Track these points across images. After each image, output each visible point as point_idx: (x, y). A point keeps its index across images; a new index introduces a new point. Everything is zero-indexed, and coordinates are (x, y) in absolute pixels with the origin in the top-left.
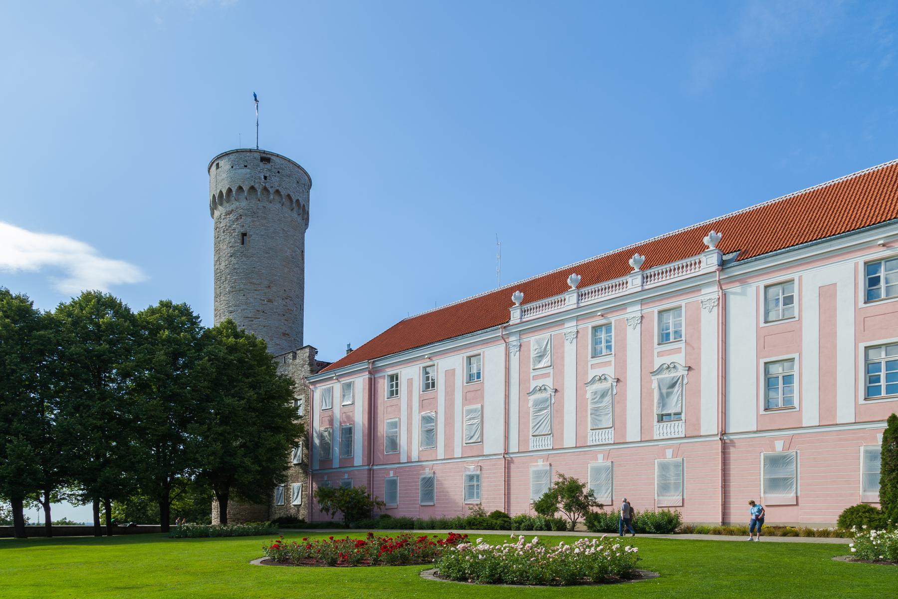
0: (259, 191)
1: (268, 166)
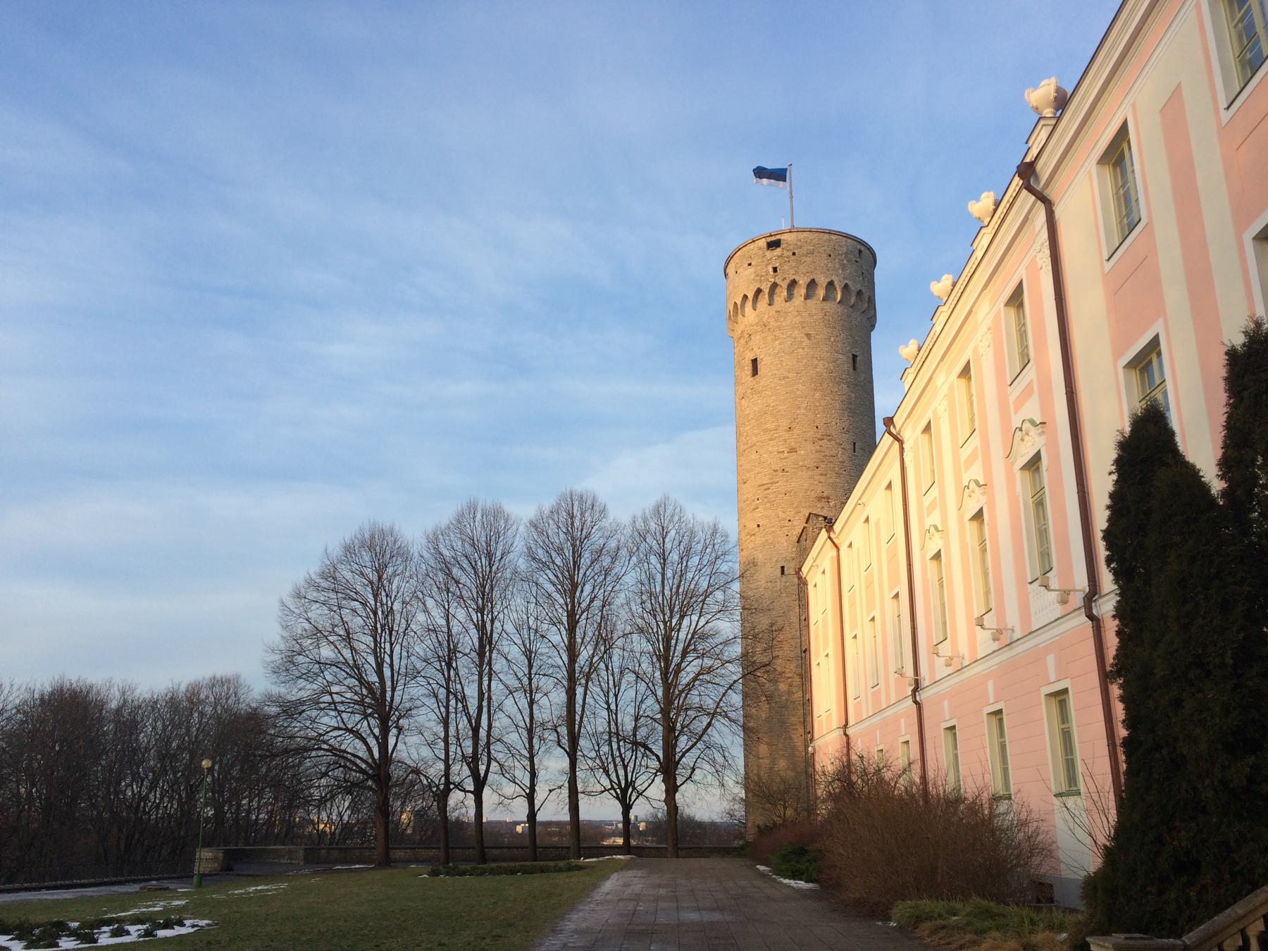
1: (778, 251)
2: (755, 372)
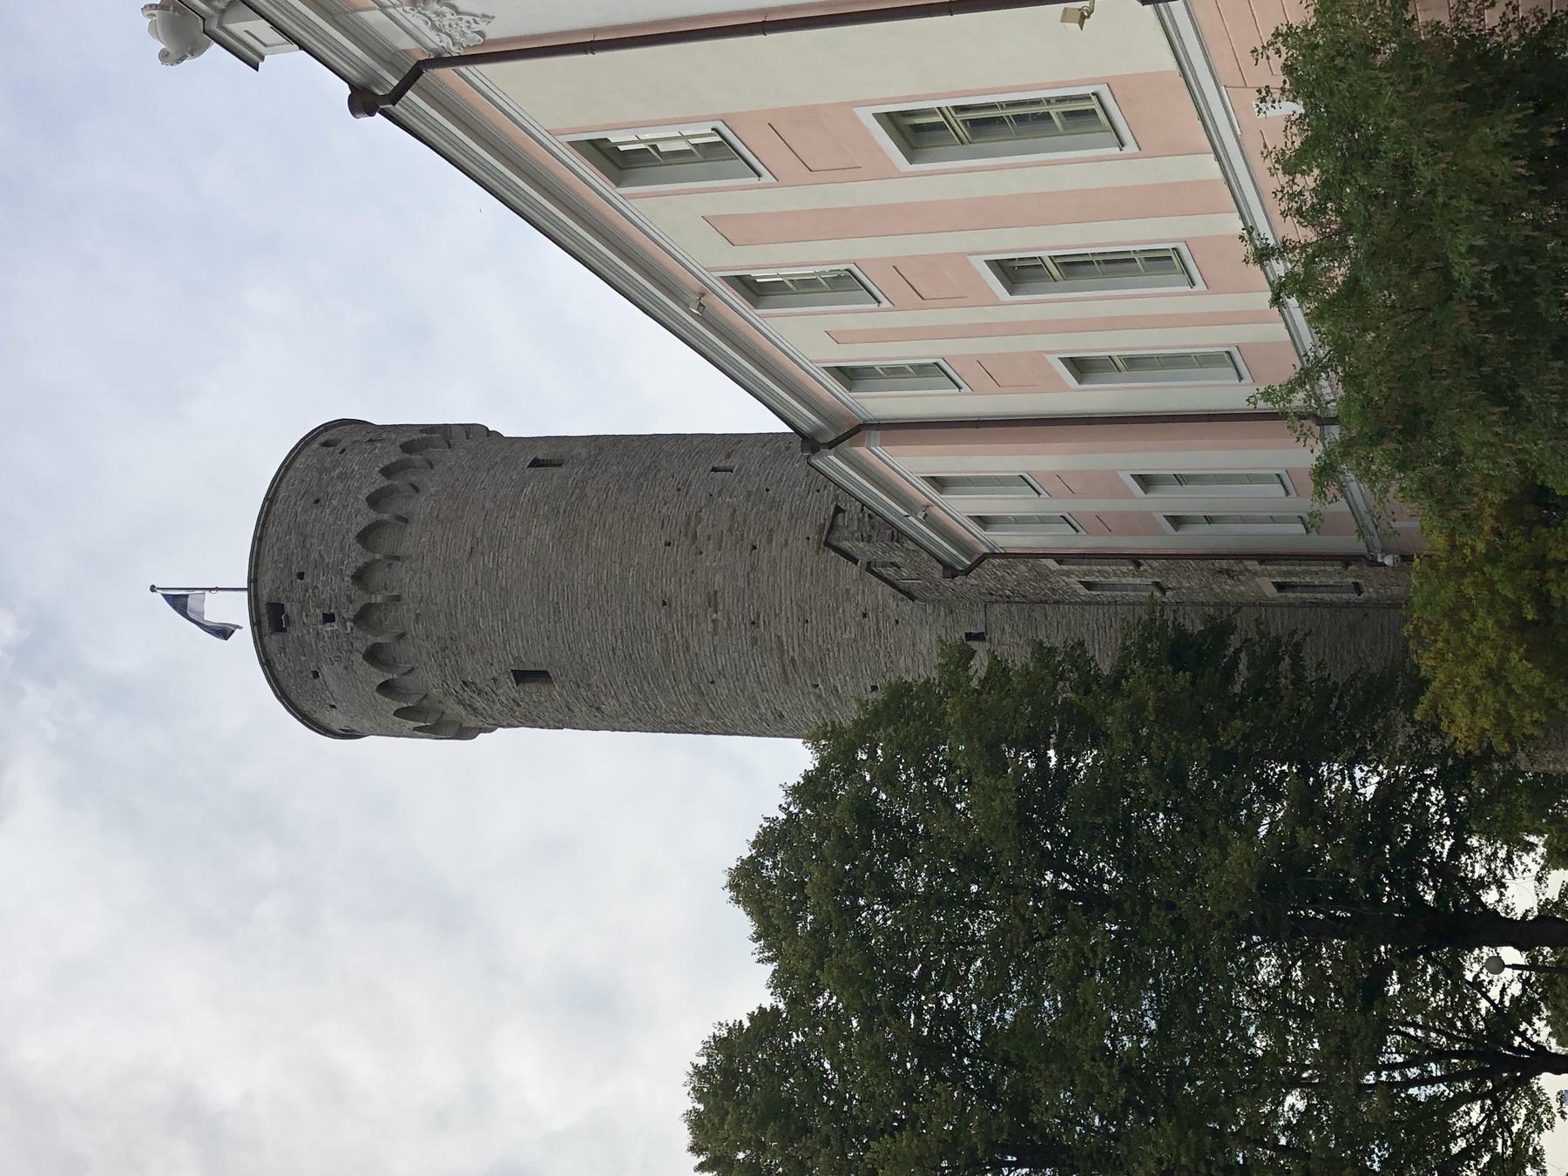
0: (372, 639)
1: (291, 609)
2: (541, 676)
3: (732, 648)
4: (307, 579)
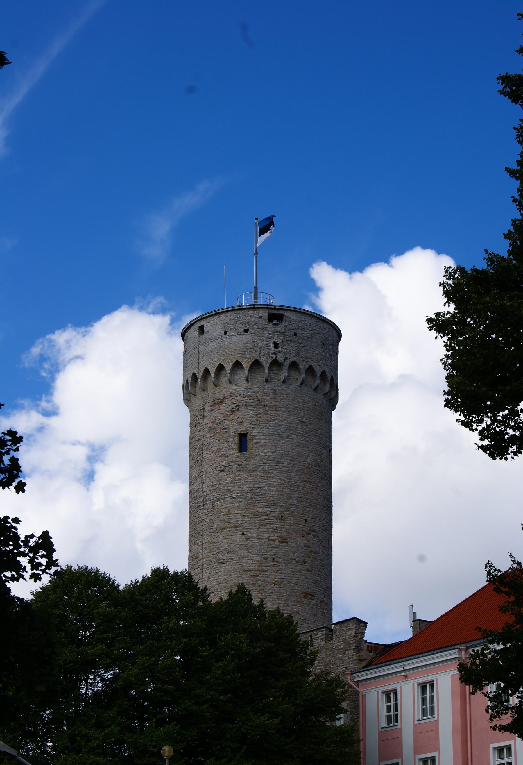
3: (262, 547)
4: (294, 338)
